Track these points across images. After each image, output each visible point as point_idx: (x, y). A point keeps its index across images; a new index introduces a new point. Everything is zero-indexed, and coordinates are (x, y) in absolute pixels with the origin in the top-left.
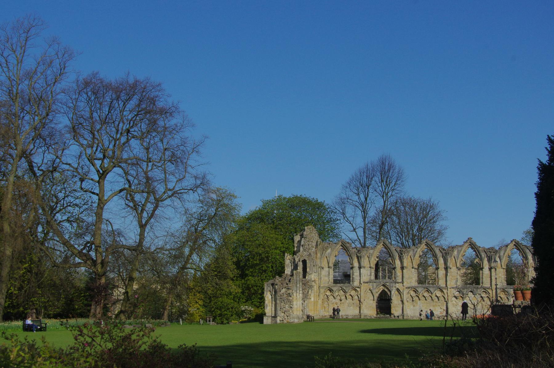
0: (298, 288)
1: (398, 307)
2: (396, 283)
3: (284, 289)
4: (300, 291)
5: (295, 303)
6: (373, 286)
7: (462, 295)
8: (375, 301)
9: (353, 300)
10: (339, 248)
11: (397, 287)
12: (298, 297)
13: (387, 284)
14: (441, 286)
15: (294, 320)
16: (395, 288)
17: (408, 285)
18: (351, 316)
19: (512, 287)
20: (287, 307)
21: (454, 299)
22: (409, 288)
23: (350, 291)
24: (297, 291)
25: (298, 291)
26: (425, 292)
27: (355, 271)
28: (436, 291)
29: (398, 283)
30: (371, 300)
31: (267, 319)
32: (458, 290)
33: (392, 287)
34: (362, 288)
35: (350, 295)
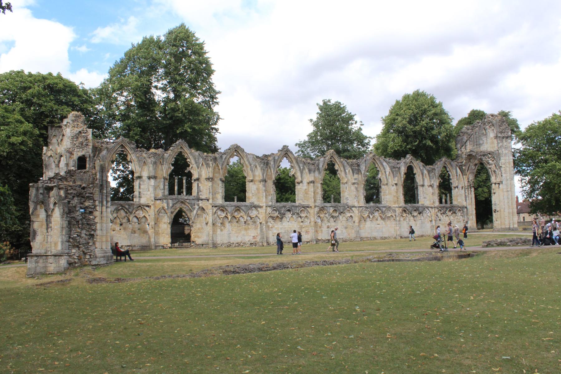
0: (105, 197)
2: (199, 199)
3: (76, 198)
4: (107, 202)
5: (98, 226)
6: (168, 204)
8: (170, 226)
9: (139, 224)
10: (118, 150)
11: (200, 205)
12: (104, 214)
13: (188, 201)
16: (197, 207)
18: (135, 246)
19: (328, 205)
20: (83, 235)
21: (271, 220)
22: (216, 206)
23: (134, 211)
24: (102, 202)
25: (105, 203)
26: (235, 212)
27: (141, 183)
29: (202, 200)
30: (165, 223)
31: (37, 262)
32: (275, 209)
33: (194, 206)
34: (152, 207)
35: (136, 216)
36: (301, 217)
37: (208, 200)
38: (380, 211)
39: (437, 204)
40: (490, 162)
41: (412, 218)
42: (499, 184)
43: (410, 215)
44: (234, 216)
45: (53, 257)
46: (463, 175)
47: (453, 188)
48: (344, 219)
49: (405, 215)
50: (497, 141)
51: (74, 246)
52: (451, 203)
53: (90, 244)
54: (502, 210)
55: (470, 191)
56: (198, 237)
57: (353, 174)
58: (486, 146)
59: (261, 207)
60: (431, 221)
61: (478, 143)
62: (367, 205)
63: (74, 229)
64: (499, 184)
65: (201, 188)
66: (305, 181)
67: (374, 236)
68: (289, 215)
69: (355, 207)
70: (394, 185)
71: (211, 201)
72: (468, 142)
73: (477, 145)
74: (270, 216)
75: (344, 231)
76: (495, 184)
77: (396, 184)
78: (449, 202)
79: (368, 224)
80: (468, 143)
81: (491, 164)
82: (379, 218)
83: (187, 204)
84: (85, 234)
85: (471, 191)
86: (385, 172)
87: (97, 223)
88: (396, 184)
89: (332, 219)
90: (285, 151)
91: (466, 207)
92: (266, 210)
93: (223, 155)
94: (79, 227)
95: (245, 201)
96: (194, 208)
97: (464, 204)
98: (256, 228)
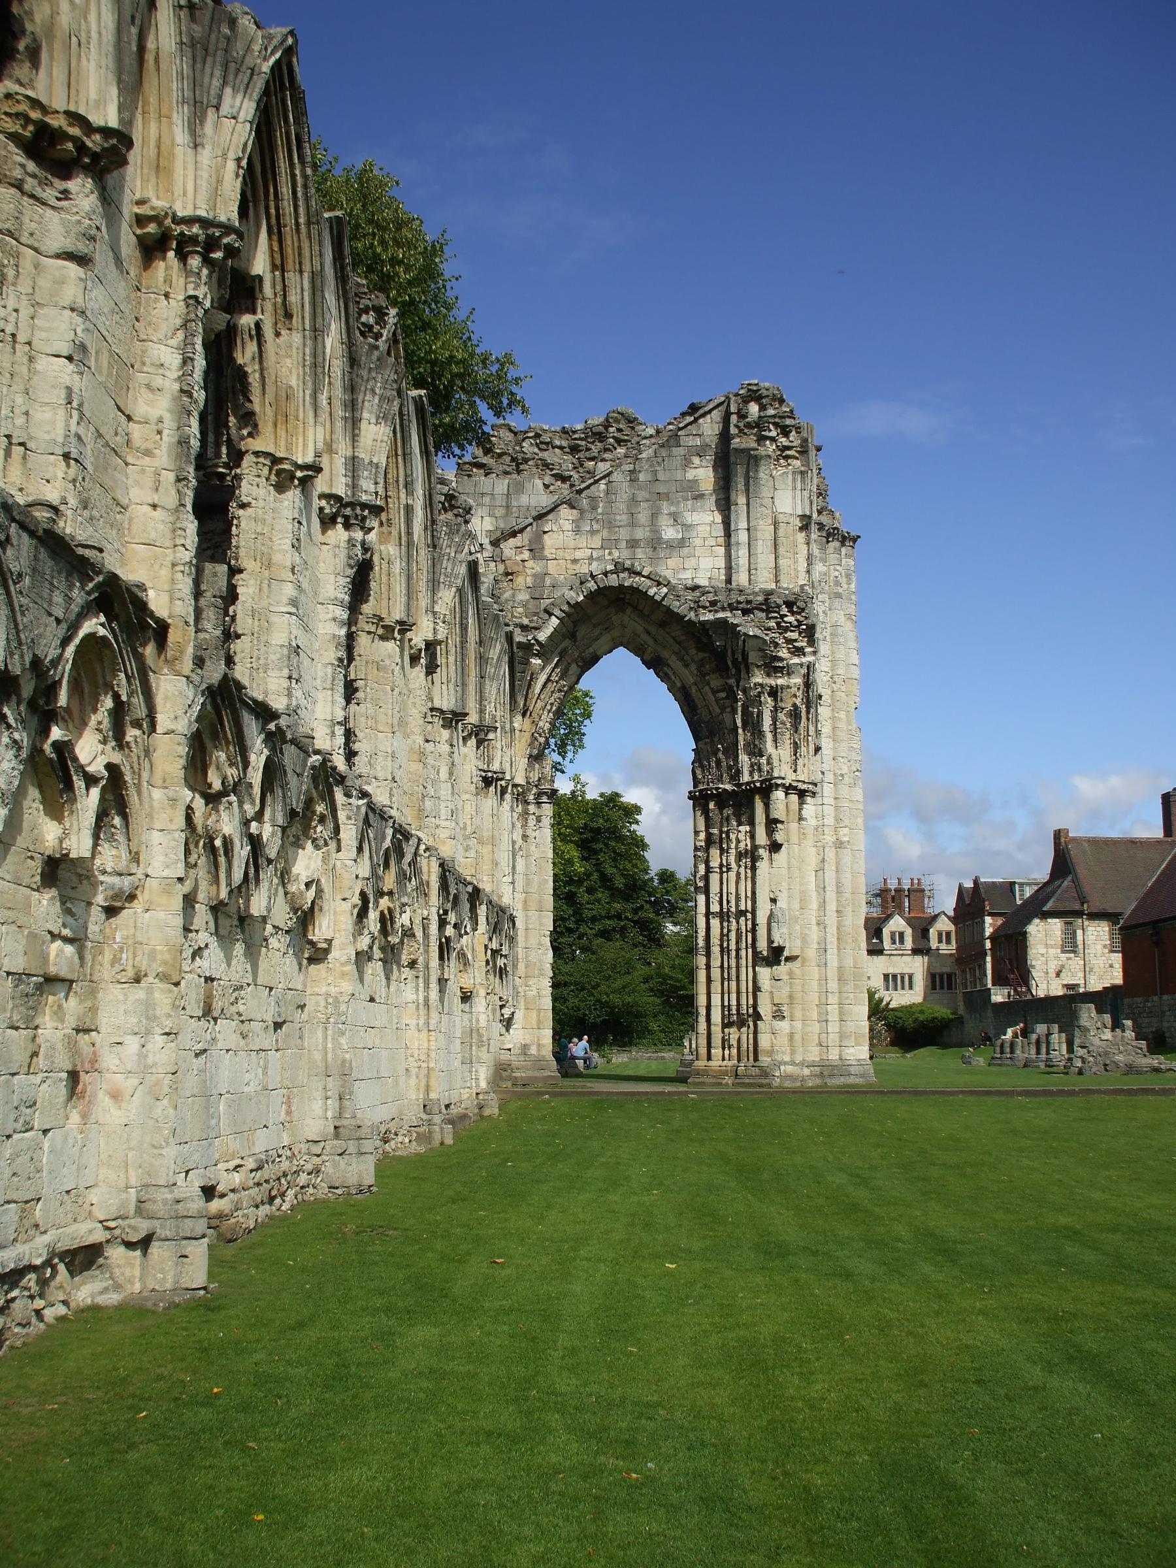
40: (784, 653)
54: (811, 953)
61: (640, 534)
64: (802, 794)
72: (565, 512)
73: (633, 544)
76: (788, 789)
80: (568, 526)
81: (788, 671)
85: (539, 820)
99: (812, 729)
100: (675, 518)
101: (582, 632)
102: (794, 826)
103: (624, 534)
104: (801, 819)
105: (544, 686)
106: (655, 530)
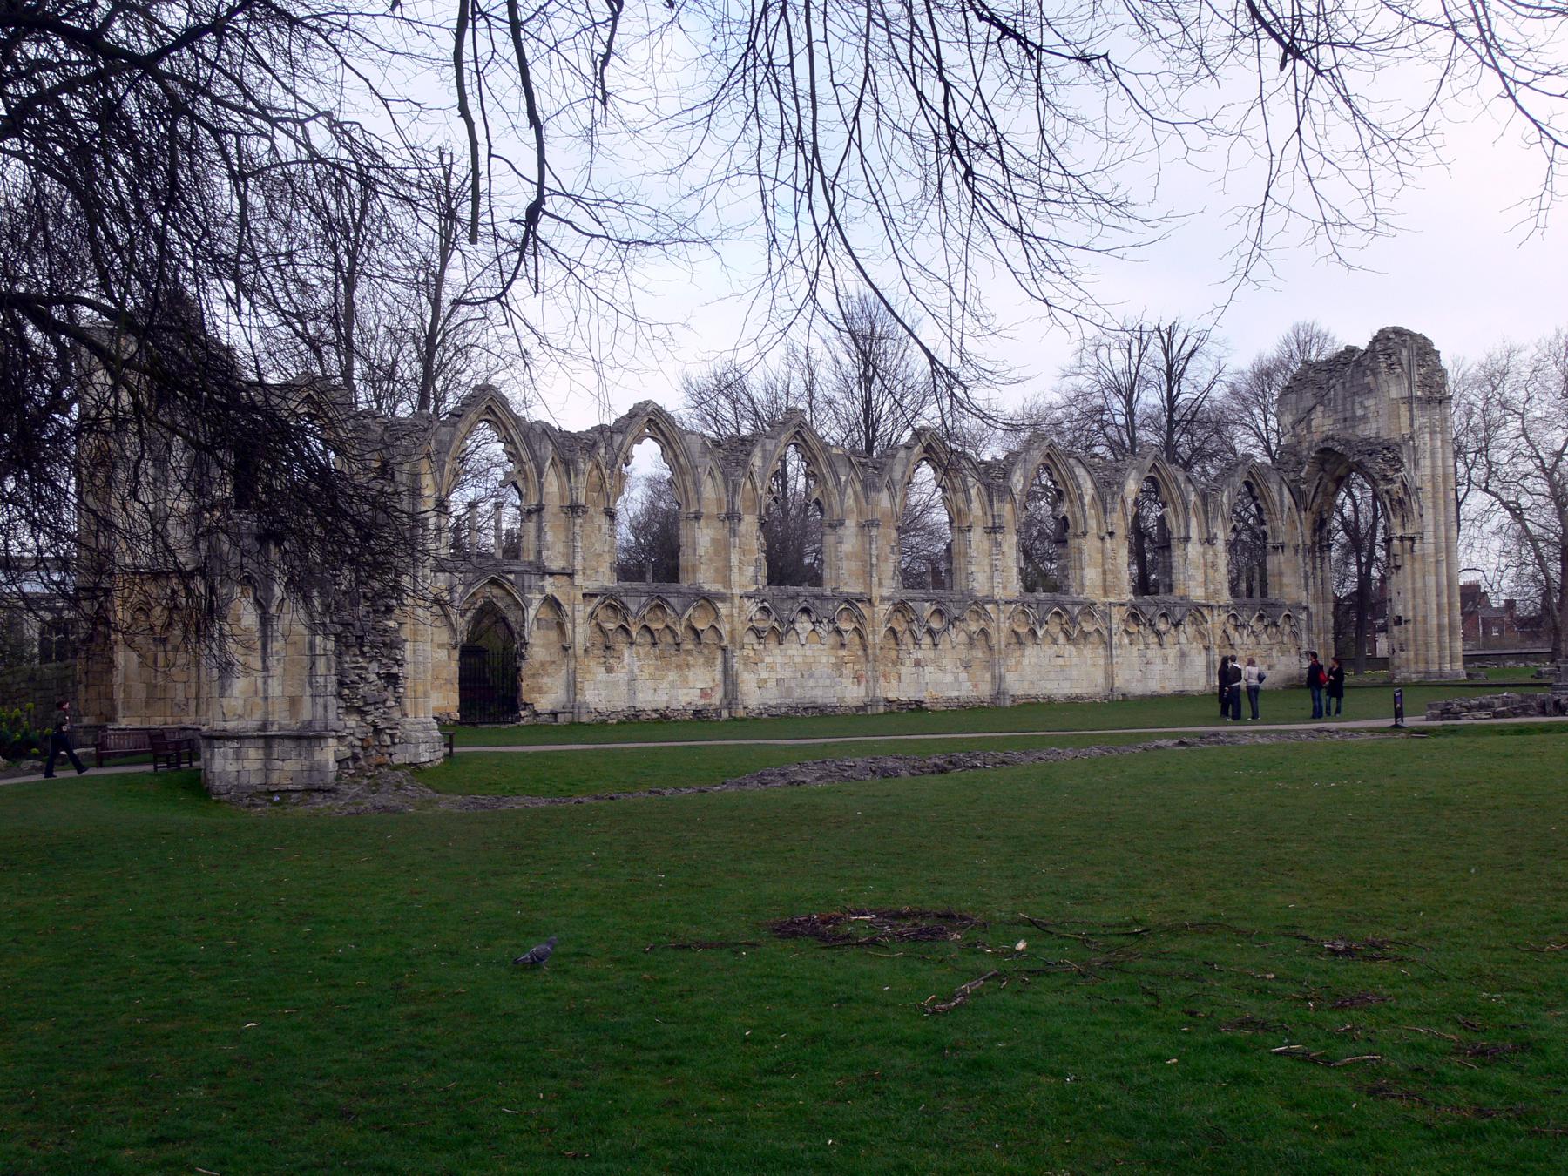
1: (549, 675)
2: (544, 572)
7: (776, 625)
8: (456, 654)
11: (549, 590)
13: (511, 577)
14: (706, 587)
15: (418, 755)
17: (591, 585)
20: (373, 677)
21: (750, 638)
22: (595, 595)
28: (691, 609)
29: (552, 574)
30: (441, 646)
32: (766, 604)
36: (839, 632)
37: (571, 575)
38: (1066, 617)
39: (1225, 597)
41: (1153, 639)
42: (1412, 539)
43: (1149, 631)
44: (645, 626)
45: (287, 743)
46: (1298, 511)
47: (1269, 547)
48: (963, 637)
49: (1133, 629)
50: (1411, 410)
51: (350, 709)
52: (1264, 593)
53: (388, 704)
55: (1318, 560)
56: (540, 690)
57: (991, 501)
58: (1374, 426)
59: (722, 598)
60: (1207, 649)
61: (1348, 415)
62: (1030, 597)
63: (348, 659)
65: (549, 537)
66: (851, 523)
67: (1046, 692)
68: (804, 625)
69: (997, 603)
70: (1107, 537)
71: (578, 580)
72: (1320, 408)
74: (752, 629)
75: (963, 676)
76: (1402, 539)
77: (1111, 534)
78: (1257, 594)
79: (1032, 656)
80: (1320, 415)
82: (1062, 638)
83: (508, 586)
84: (378, 674)
86: (1081, 496)
87: (406, 641)
88: (1111, 534)
89: (927, 640)
90: (795, 426)
91: (1306, 608)
92: (741, 609)
93: (615, 436)
94: (363, 654)
95: (678, 582)
96: (529, 603)
97: (1303, 597)
98: (710, 663)
99: (1415, 506)
100: (1361, 403)
101: (1327, 467)
102: (1407, 556)
103: (1340, 416)
104: (1412, 551)
105: (1314, 497)
106: (1354, 412)
